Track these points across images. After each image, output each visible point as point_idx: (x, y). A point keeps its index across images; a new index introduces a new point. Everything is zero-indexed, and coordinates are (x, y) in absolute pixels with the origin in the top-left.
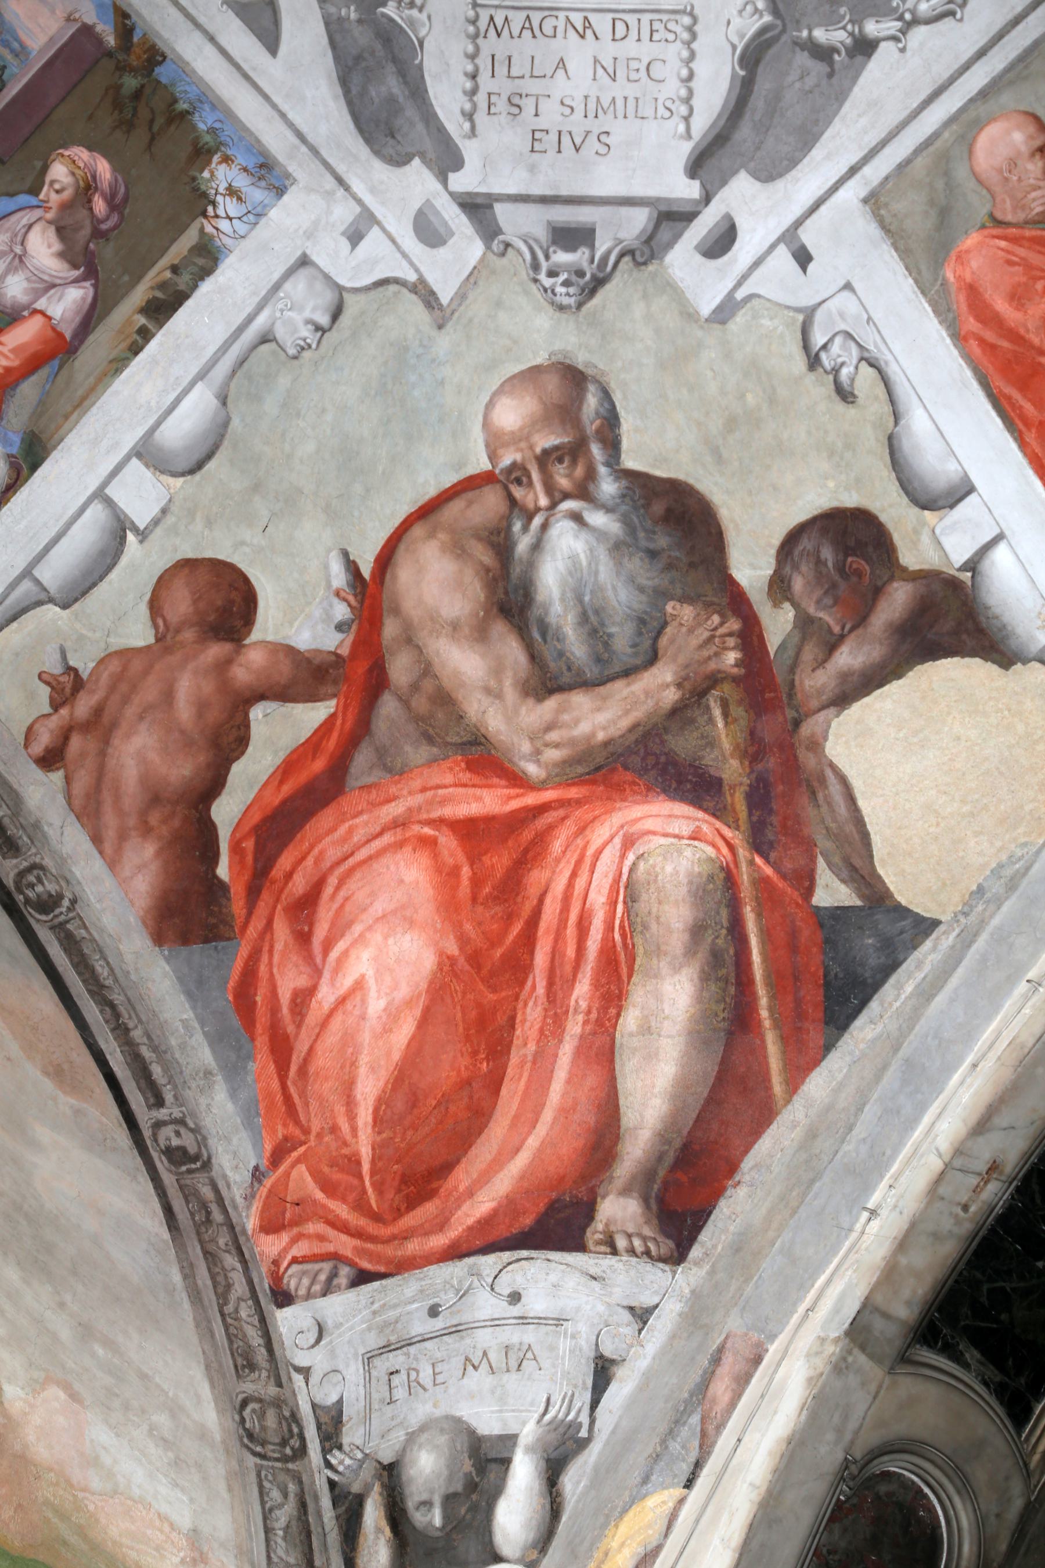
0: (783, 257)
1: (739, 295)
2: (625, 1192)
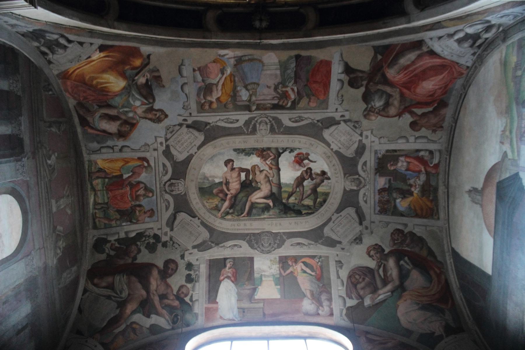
0: (338, 111)
1: (344, 111)
2: (422, 50)
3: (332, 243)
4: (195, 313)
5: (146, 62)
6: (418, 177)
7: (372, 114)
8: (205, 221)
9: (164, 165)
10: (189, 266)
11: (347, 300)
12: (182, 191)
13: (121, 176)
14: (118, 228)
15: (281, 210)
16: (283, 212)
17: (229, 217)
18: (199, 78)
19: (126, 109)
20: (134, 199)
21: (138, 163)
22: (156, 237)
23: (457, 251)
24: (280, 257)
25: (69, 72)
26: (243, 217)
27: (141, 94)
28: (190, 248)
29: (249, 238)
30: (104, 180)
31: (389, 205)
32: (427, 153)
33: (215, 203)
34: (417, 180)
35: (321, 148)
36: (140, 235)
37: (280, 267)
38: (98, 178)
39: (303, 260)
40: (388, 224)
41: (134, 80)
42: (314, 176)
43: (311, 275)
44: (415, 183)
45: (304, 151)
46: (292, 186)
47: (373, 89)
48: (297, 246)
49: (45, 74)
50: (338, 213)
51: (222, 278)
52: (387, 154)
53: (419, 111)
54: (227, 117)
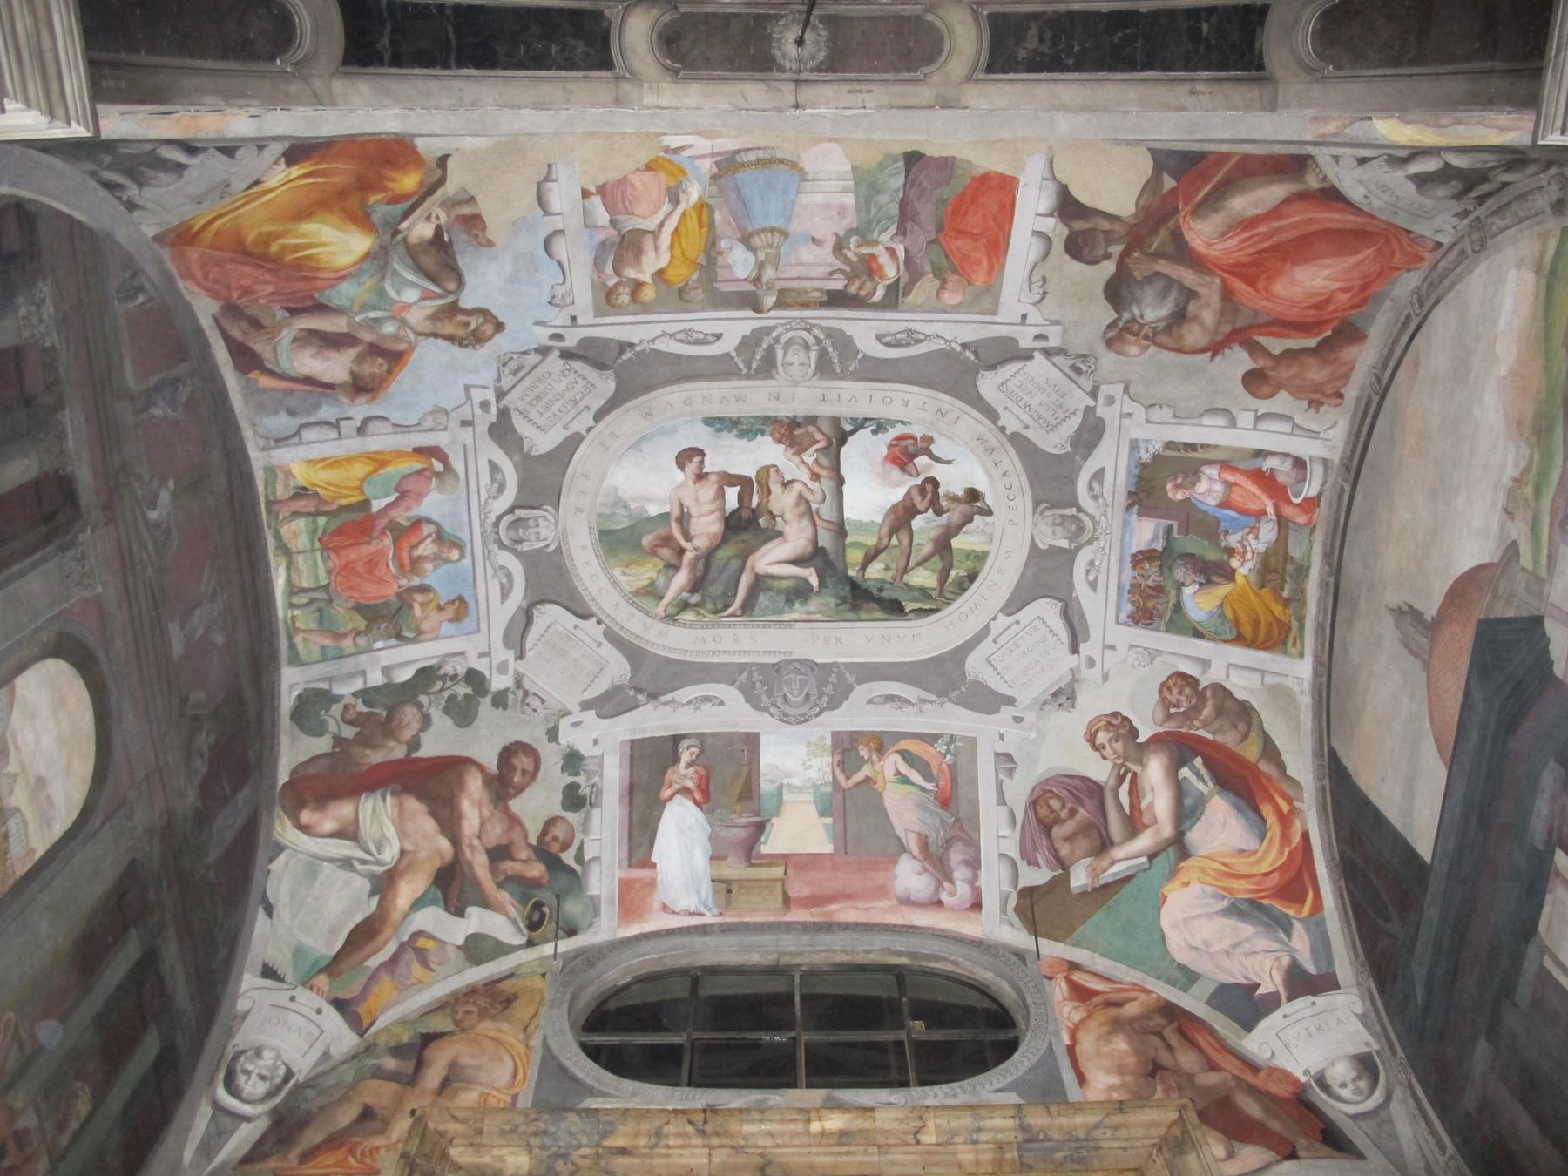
3: (988, 701)
4: (591, 897)
5: (434, 179)
6: (1254, 530)
7: (1132, 338)
8: (617, 629)
9: (494, 468)
10: (573, 760)
11: (1023, 866)
12: (550, 539)
13: (366, 504)
14: (363, 657)
15: (844, 600)
16: (847, 606)
17: (689, 616)
18: (602, 217)
19: (372, 315)
20: (408, 568)
21: (416, 465)
22: (475, 679)
23: (1345, 761)
24: (835, 734)
25: (193, 226)
26: (732, 615)
27: (420, 269)
28: (573, 705)
29: (747, 679)
30: (315, 523)
31: (1161, 601)
32: (1289, 463)
33: (648, 575)
34: (1251, 536)
35: (970, 421)
36: (426, 676)
37: (835, 764)
38: (296, 515)
39: (904, 745)
40: (1153, 655)
41: (396, 232)
42: (944, 503)
43: (923, 789)
44: (1244, 547)
45: (917, 431)
46: (876, 529)
47: (1140, 269)
48: (887, 706)
49: (118, 245)
50: (1010, 615)
51: (666, 793)
52: (1168, 453)
53: (1276, 345)
54: (688, 325)
